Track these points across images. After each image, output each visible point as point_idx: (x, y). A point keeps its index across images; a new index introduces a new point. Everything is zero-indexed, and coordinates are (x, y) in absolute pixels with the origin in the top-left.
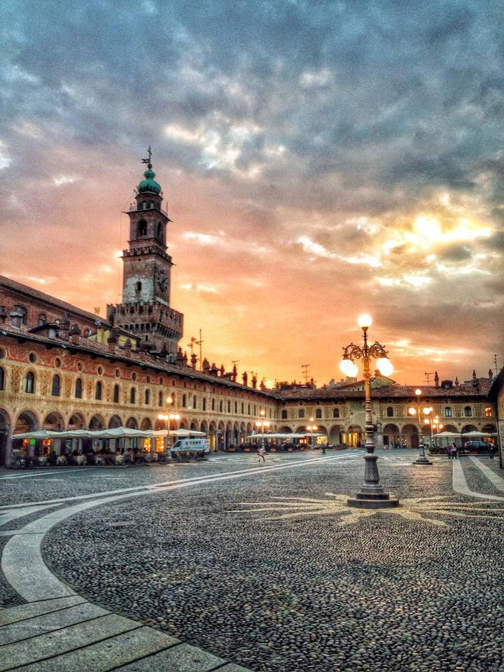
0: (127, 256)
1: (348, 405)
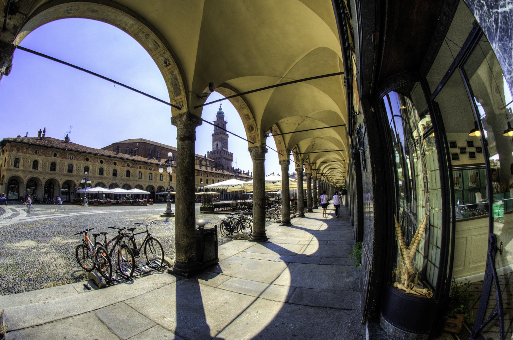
0: (213, 135)
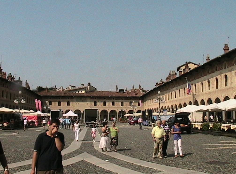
1: (74, 100)
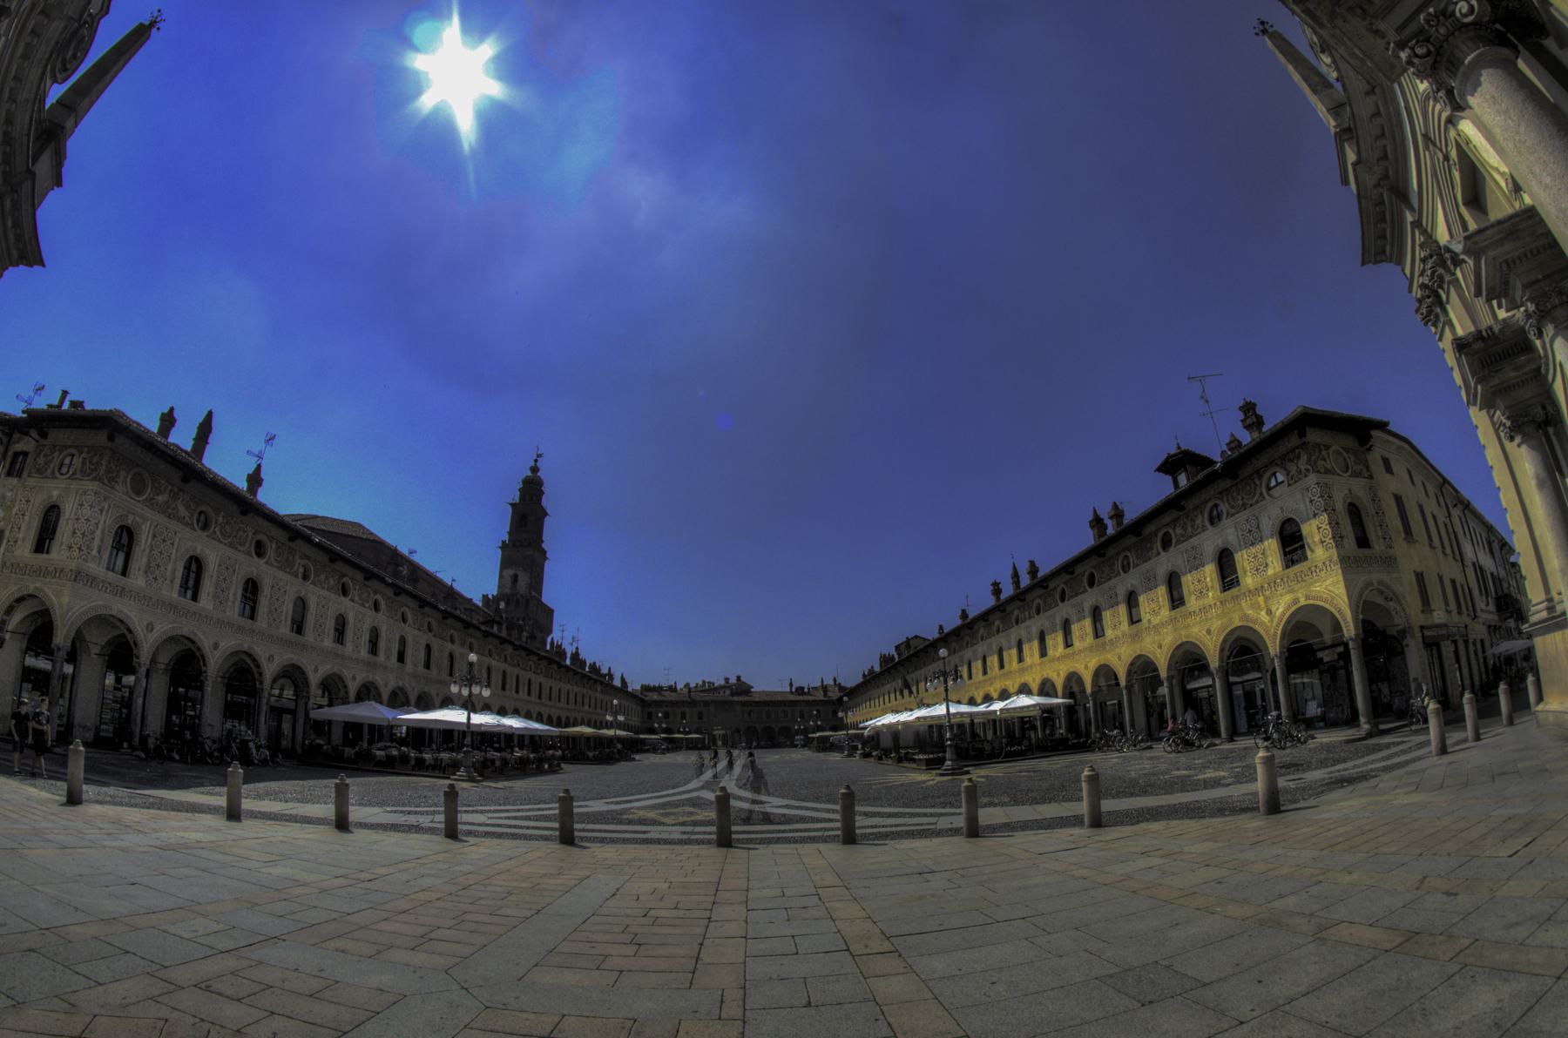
0: (504, 546)
